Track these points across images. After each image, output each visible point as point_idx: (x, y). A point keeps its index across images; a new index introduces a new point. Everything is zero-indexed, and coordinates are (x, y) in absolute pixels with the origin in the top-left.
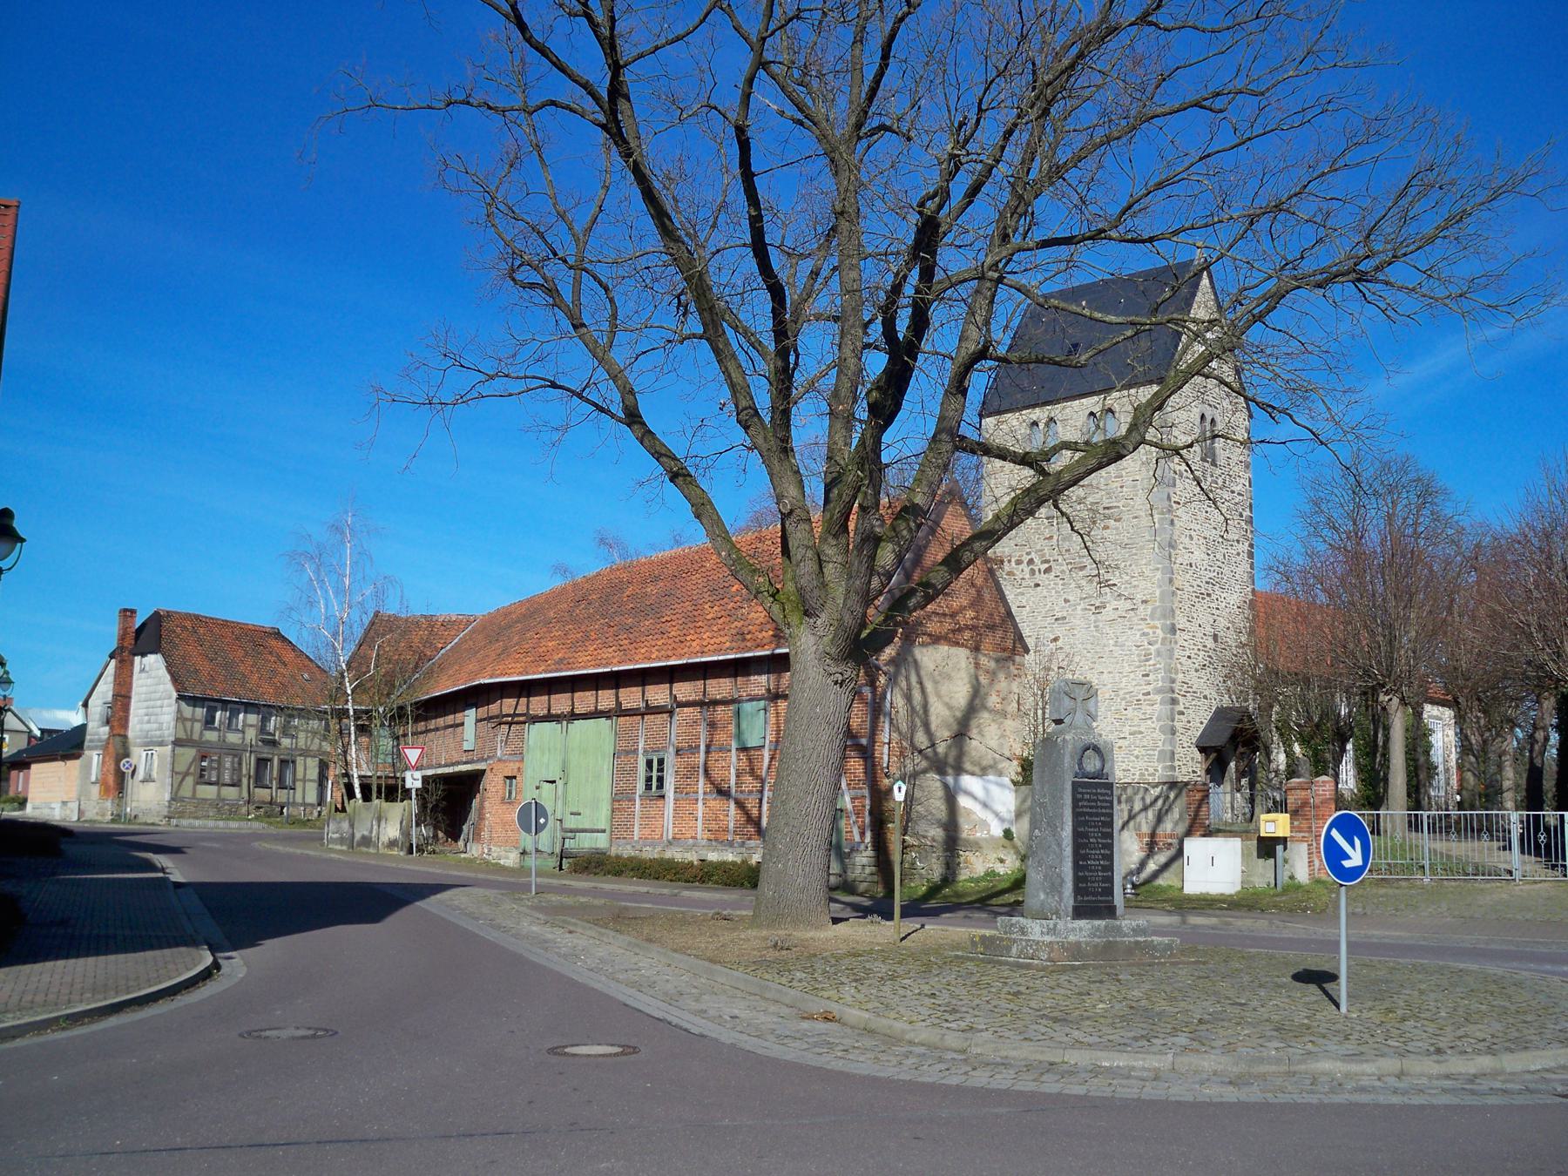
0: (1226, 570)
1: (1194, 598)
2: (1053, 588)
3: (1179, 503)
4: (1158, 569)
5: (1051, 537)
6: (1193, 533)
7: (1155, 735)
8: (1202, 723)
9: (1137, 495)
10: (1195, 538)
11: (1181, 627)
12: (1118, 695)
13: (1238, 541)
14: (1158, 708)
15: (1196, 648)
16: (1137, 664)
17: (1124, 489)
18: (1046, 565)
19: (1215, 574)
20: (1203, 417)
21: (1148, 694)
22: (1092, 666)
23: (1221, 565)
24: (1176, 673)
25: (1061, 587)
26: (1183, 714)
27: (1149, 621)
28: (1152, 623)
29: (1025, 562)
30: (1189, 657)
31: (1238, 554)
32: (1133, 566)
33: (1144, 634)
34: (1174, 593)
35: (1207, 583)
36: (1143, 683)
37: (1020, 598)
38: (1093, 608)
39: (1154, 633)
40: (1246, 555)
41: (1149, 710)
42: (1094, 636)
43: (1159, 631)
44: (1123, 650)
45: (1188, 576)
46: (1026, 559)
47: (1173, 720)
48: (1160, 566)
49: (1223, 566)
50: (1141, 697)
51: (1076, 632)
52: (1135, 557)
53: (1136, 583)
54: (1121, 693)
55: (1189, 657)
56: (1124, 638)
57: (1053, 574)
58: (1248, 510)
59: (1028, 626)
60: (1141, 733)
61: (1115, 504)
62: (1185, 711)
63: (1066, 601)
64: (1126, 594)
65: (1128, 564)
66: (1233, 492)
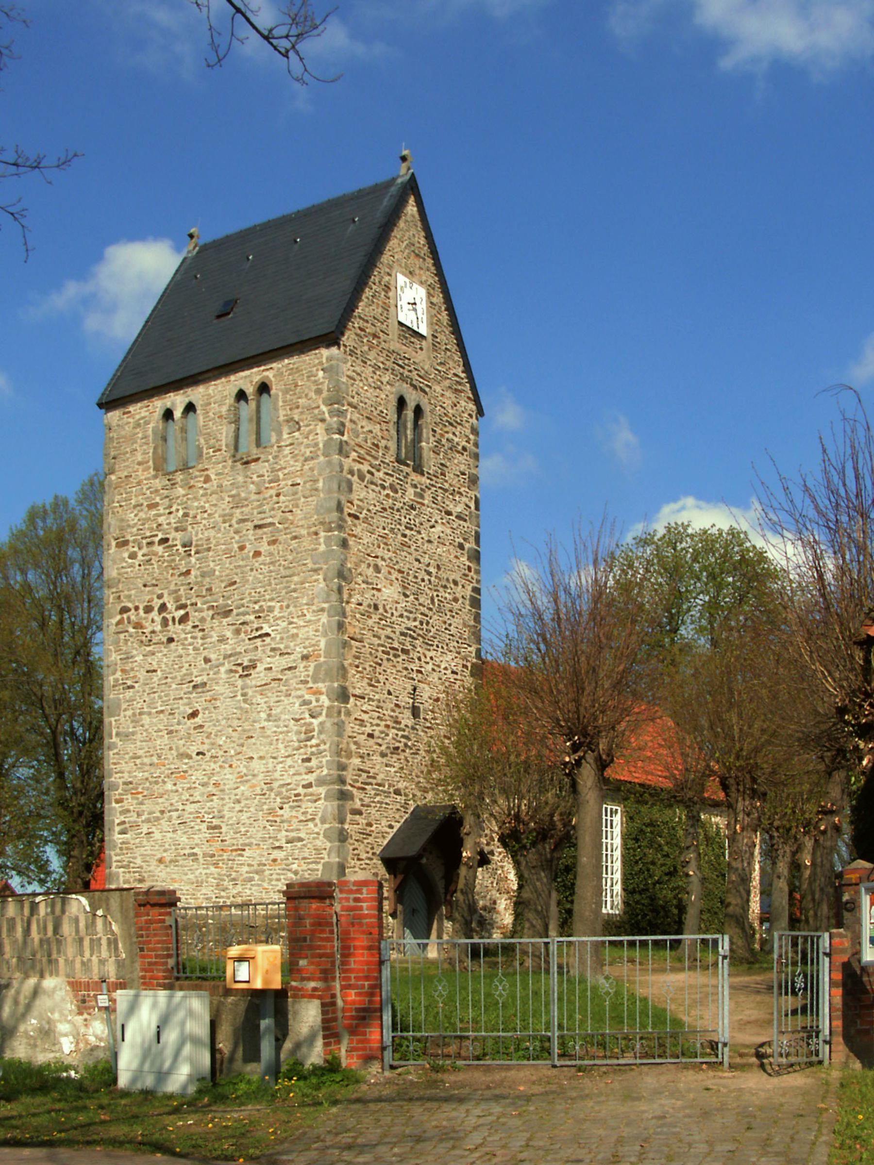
0: (435, 619)
1: (380, 654)
2: (190, 644)
3: (357, 518)
4: (323, 610)
5: (188, 572)
6: (380, 563)
7: (318, 843)
8: (391, 827)
9: (297, 506)
10: (384, 570)
11: (357, 692)
12: (271, 790)
13: (455, 583)
14: (326, 806)
15: (383, 723)
16: (296, 744)
17: (282, 498)
18: (182, 612)
19: (417, 623)
20: (401, 402)
21: (309, 785)
22: (239, 749)
23: (427, 612)
24: (349, 756)
25: (200, 641)
26: (360, 813)
27: (310, 685)
28: (315, 686)
29: (156, 609)
30: (371, 736)
31: (456, 600)
32: (291, 608)
33: (305, 703)
34: (345, 644)
35: (402, 634)
36: (303, 771)
37: (149, 660)
38: (240, 669)
39: (317, 700)
40: (467, 602)
41: (310, 808)
42: (241, 708)
43: (324, 699)
44: (278, 727)
45: (370, 622)
46: (157, 603)
47: (342, 821)
48: (326, 605)
49: (430, 614)
50: (300, 790)
51: (218, 703)
52: (294, 595)
53: (295, 631)
54: (275, 785)
55: (371, 736)
56: (279, 710)
57: (190, 623)
58: (472, 539)
59: (160, 697)
60: (300, 840)
61: (270, 520)
62: (364, 809)
63: (207, 660)
64: (282, 646)
65: (285, 604)
66: (449, 513)
